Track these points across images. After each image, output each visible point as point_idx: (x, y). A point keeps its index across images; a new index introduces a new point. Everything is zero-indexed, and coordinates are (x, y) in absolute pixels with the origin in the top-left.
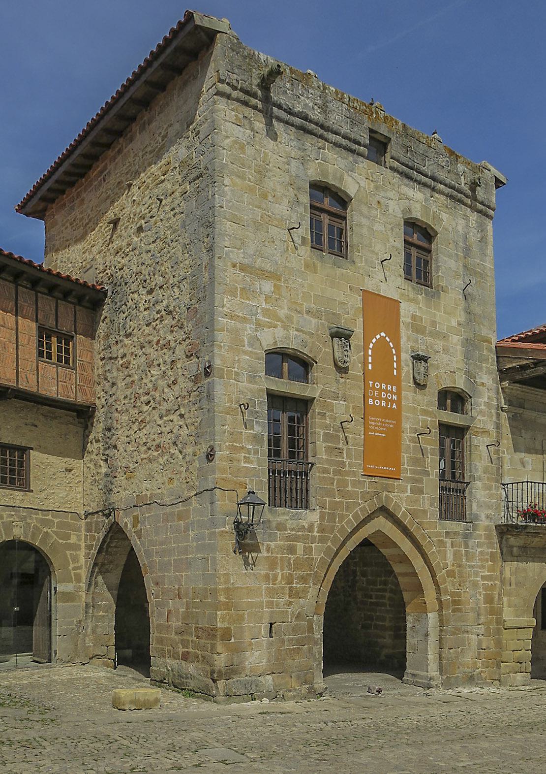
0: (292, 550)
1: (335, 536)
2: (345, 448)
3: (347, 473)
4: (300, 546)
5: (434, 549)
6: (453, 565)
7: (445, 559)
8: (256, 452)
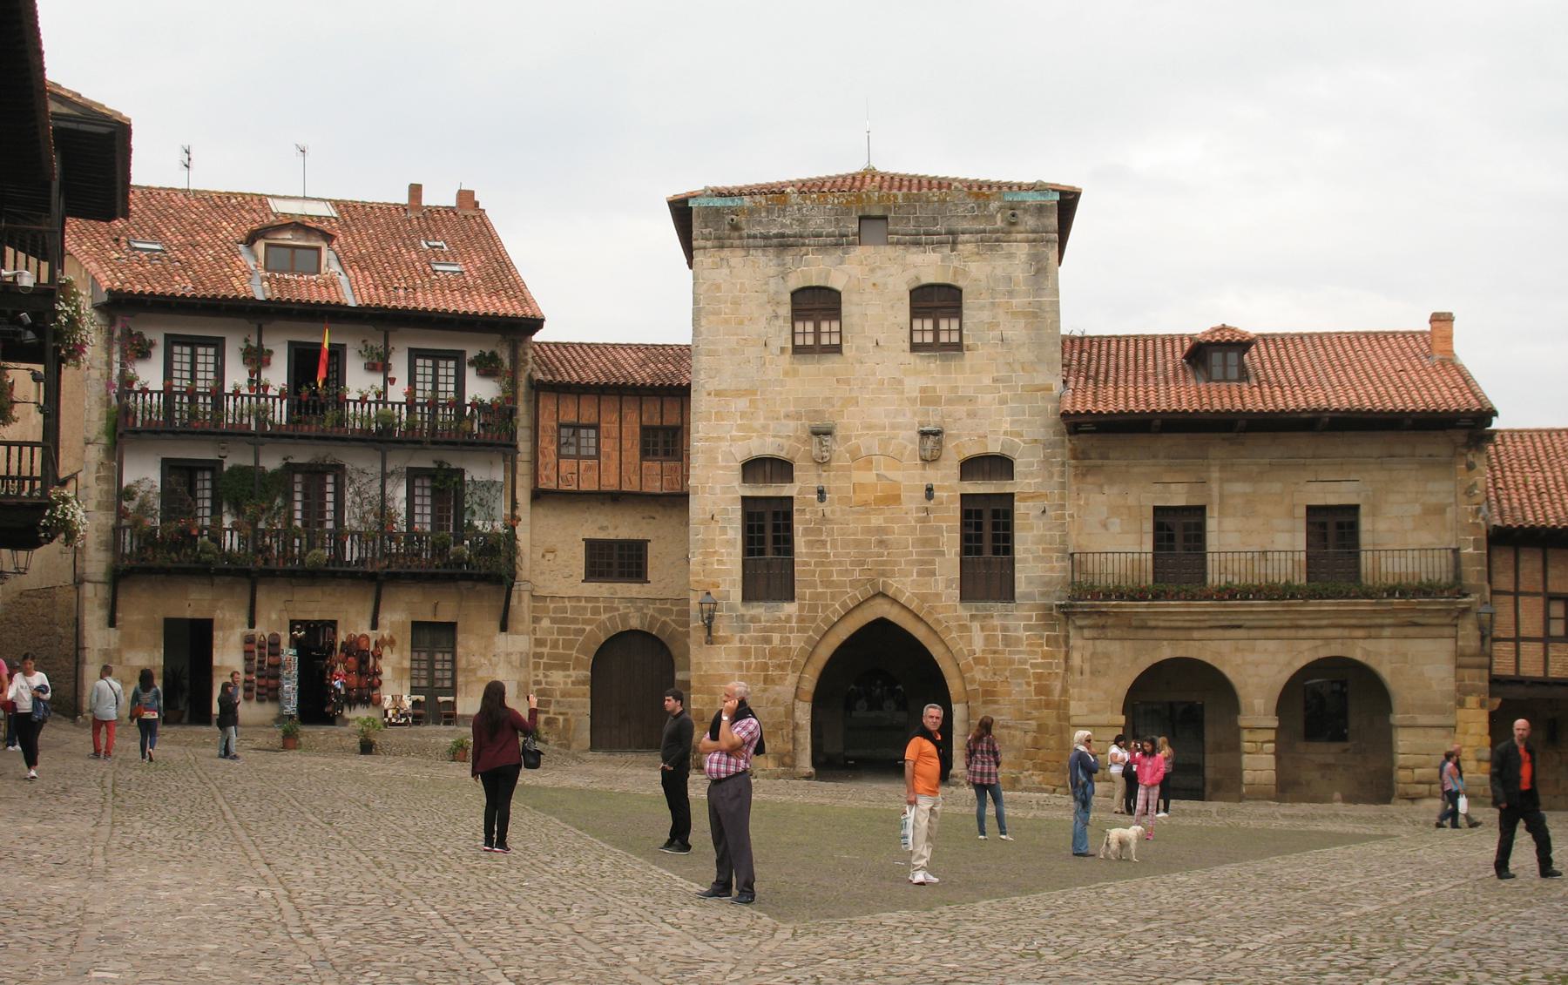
0: (768, 640)
1: (818, 626)
3: (831, 564)
4: (776, 637)
5: (954, 635)
7: (970, 642)
8: (729, 554)
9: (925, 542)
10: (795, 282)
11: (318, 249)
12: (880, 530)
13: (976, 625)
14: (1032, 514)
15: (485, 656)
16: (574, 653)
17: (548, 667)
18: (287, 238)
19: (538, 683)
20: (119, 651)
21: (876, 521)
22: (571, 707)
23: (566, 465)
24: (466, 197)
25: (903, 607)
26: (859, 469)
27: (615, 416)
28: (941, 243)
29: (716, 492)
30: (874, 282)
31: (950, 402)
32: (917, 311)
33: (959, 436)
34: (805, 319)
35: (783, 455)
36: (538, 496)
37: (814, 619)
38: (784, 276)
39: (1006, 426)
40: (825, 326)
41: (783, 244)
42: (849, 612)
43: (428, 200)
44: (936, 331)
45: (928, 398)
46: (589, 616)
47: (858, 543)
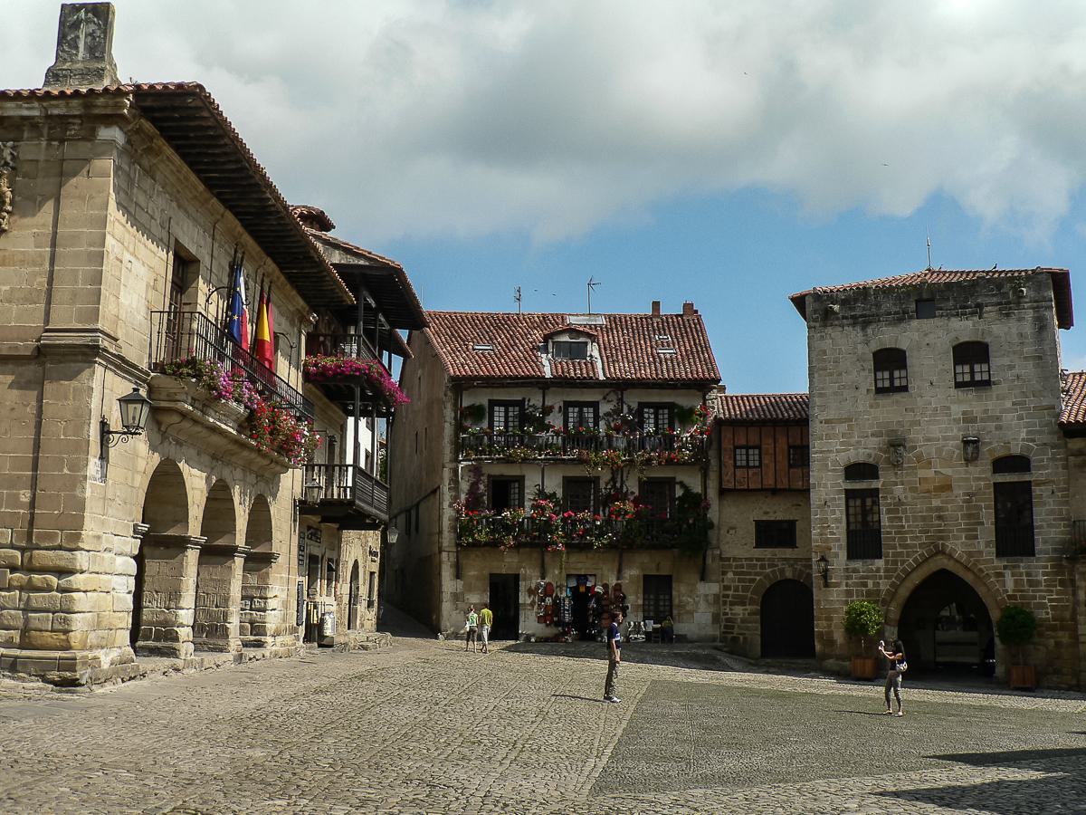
0: (865, 585)
2: (904, 516)
3: (906, 532)
4: (870, 583)
6: (1014, 591)
9: (969, 516)
10: (875, 346)
11: (586, 343)
12: (939, 509)
13: (1008, 573)
14: (1045, 494)
15: (691, 597)
16: (749, 594)
17: (732, 604)
18: (565, 338)
19: (726, 614)
20: (463, 594)
21: (936, 503)
22: (747, 629)
23: (738, 472)
24: (688, 307)
25: (957, 561)
26: (923, 468)
27: (771, 441)
28: (973, 314)
29: (827, 485)
30: (929, 343)
31: (982, 420)
32: (958, 360)
33: (990, 443)
34: (883, 370)
35: (871, 461)
36: (723, 492)
37: (896, 570)
38: (867, 343)
39: (1023, 435)
40: (896, 374)
41: (864, 322)
42: (919, 565)
43: (664, 311)
44: (972, 373)
45: (969, 419)
46: (758, 570)
47: (924, 518)
